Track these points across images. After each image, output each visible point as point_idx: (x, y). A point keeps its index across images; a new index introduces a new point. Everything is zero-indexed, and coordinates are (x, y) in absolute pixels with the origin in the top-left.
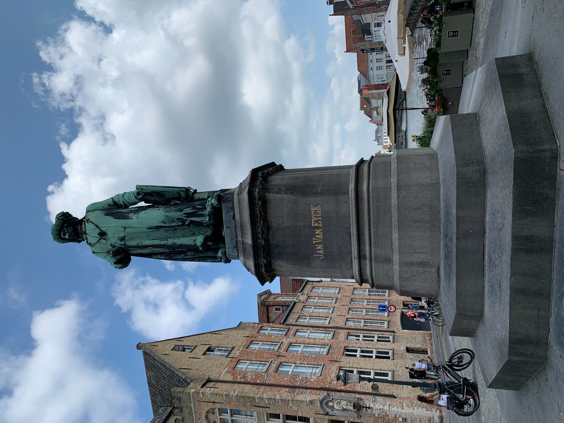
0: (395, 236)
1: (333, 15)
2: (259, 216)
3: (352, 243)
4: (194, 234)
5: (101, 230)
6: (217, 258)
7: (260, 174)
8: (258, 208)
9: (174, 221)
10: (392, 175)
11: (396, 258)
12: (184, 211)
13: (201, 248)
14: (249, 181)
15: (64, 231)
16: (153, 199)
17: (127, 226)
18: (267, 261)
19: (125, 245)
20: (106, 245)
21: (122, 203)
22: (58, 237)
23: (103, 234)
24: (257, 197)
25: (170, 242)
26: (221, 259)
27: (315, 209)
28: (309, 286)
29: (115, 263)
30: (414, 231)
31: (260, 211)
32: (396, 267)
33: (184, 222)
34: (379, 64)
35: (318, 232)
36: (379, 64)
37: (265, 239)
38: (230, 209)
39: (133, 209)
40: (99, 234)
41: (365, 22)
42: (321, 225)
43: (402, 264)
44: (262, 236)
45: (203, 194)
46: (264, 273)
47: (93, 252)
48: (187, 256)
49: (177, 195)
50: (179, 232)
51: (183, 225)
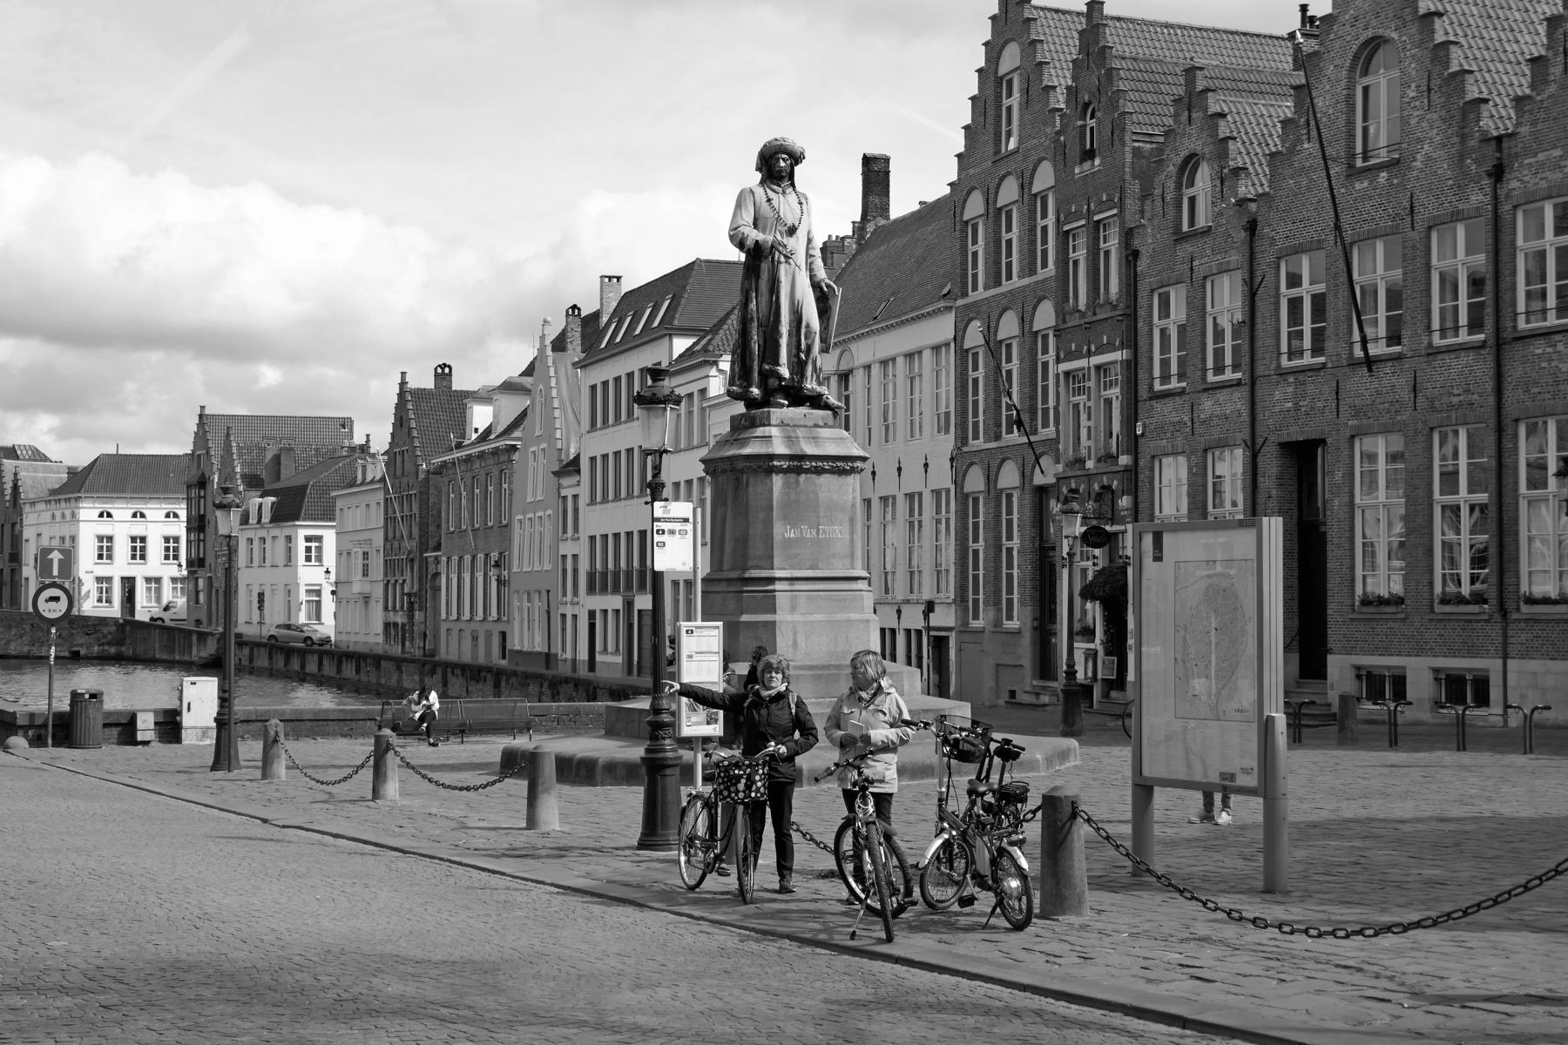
0: (819, 617)
1: (403, 384)
11: (797, 617)
32: (789, 618)
34: (122, 549)
36: (122, 549)
41: (339, 504)
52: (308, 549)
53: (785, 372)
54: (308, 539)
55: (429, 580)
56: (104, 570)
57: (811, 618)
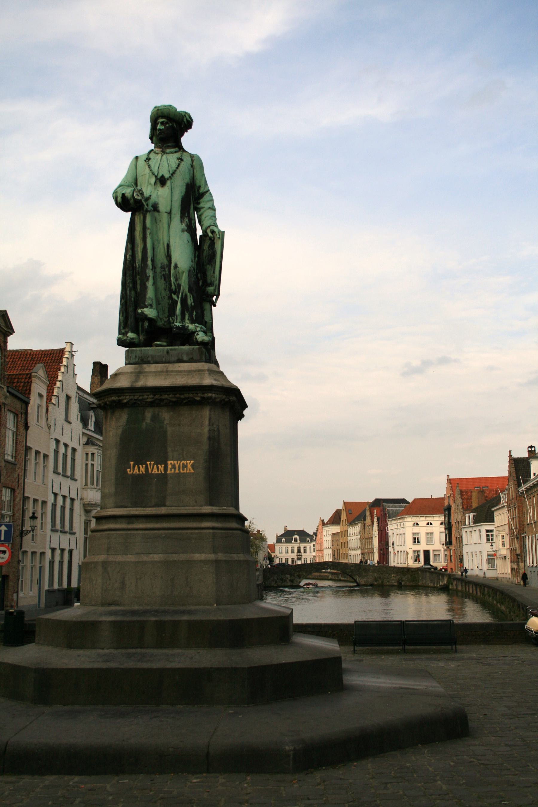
0: (156, 557)
1: (510, 456)
2: (182, 396)
3: (147, 509)
4: (158, 303)
5: (168, 179)
6: (124, 328)
7: (233, 398)
8: (191, 395)
9: (176, 279)
10: (226, 554)
11: (131, 558)
12: (188, 294)
13: (140, 311)
14: (225, 384)
15: (167, 123)
16: (206, 247)
17: (173, 216)
18: (125, 404)
19: (147, 211)
20: (148, 189)
21: (201, 205)
22: (160, 114)
23: (162, 181)
24: (206, 395)
25: (150, 273)
26: (123, 334)
27: (189, 466)
28: (19, 405)
29: (123, 195)
30: (162, 577)
31: (188, 398)
33: (176, 292)
35: (161, 468)
37: (152, 403)
38: (190, 357)
39: (193, 222)
40: (163, 176)
41: (495, 513)
42: (169, 472)
44: (157, 399)
45: (209, 315)
46: (110, 399)
47: (137, 158)
48: (130, 291)
49: (209, 281)
50: (161, 283)
51: (171, 291)
52: (488, 536)
54: (488, 531)
55: (523, 547)
56: (416, 547)
57: (145, 558)
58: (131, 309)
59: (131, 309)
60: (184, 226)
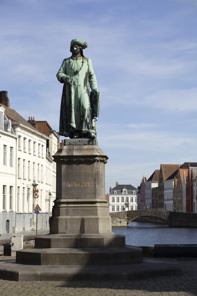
11: (68, 217)
32: (65, 217)
35: (79, 185)
43: (66, 219)
53: (74, 125)
58: (64, 123)
59: (64, 123)
60: (85, 91)
